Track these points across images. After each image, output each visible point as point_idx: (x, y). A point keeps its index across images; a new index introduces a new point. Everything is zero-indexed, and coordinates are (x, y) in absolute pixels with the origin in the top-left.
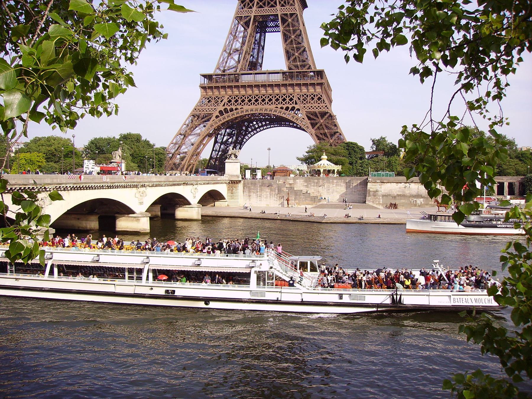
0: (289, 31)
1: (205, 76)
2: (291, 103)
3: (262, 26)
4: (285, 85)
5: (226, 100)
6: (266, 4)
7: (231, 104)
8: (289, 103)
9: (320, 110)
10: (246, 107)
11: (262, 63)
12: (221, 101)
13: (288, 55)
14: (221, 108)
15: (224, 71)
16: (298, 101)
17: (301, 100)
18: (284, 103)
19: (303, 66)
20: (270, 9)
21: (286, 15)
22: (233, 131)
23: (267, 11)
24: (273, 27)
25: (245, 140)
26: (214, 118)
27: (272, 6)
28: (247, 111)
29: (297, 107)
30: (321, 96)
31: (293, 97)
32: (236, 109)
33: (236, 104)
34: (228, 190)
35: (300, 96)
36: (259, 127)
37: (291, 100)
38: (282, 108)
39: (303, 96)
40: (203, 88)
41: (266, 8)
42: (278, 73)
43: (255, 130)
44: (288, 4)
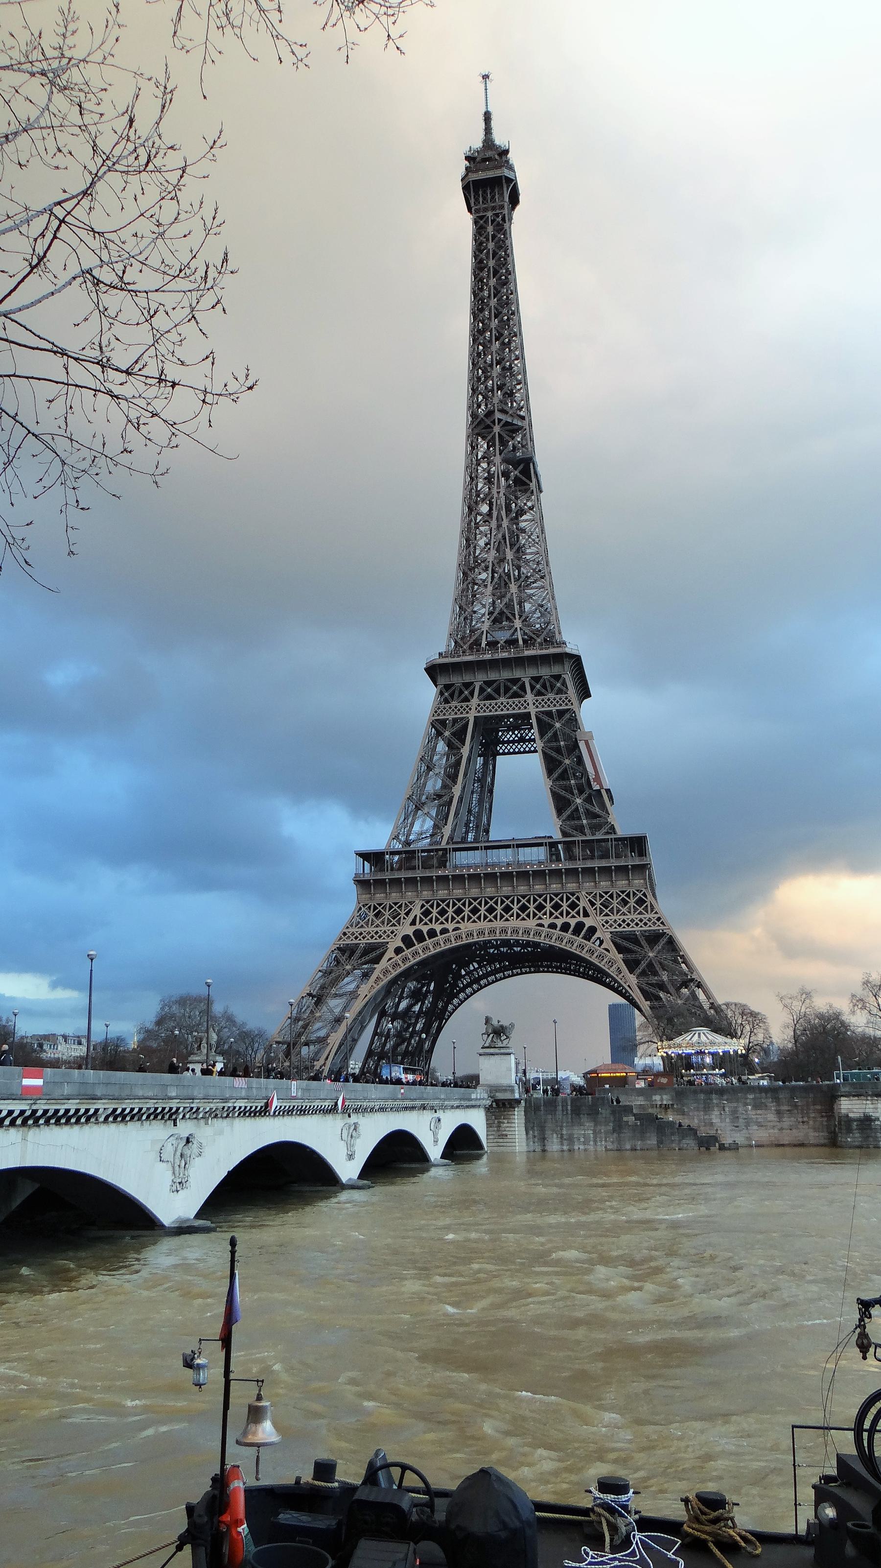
0: (558, 750)
1: (365, 856)
2: (573, 913)
3: (490, 738)
4: (556, 873)
5: (417, 911)
6: (502, 691)
8: (568, 913)
10: (466, 927)
11: (489, 825)
12: (407, 914)
13: (561, 803)
15: (408, 843)
17: (598, 905)
18: (556, 914)
19: (595, 828)
20: (511, 701)
21: (549, 714)
22: (422, 987)
23: (504, 706)
24: (513, 742)
25: (450, 1007)
26: (390, 953)
27: (516, 695)
28: (470, 934)
29: (588, 922)
30: (644, 895)
31: (578, 898)
33: (442, 919)
34: (489, 1126)
35: (595, 897)
36: (485, 976)
37: (573, 906)
38: (553, 926)
40: (362, 883)
41: (502, 699)
42: (540, 845)
43: (477, 983)
44: (552, 690)
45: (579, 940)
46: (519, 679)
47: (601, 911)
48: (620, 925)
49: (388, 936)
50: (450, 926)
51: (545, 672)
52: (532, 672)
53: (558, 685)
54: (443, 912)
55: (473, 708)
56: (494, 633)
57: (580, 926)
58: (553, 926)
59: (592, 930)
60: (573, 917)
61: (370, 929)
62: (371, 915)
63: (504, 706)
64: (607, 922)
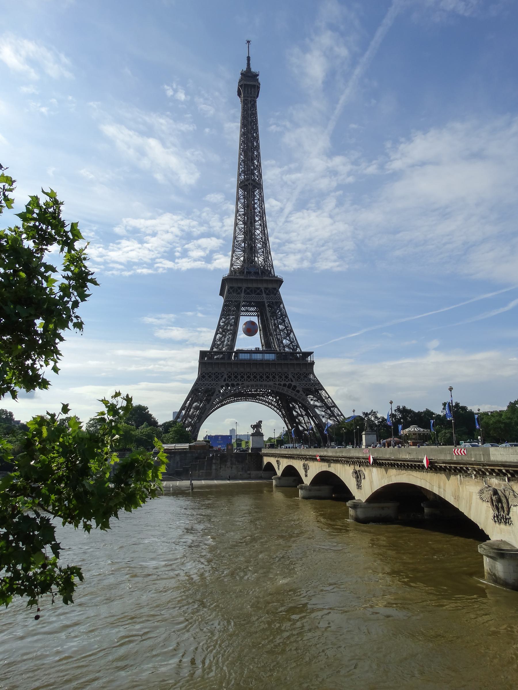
5: (226, 376)
7: (232, 380)
8: (285, 380)
12: (222, 377)
17: (296, 378)
27: (258, 294)
29: (293, 384)
31: (288, 374)
33: (236, 380)
39: (297, 374)
41: (253, 295)
47: (298, 380)
50: (240, 383)
51: (270, 286)
52: (265, 285)
54: (236, 377)
58: (280, 385)
61: (207, 382)
62: (207, 377)
63: (254, 297)
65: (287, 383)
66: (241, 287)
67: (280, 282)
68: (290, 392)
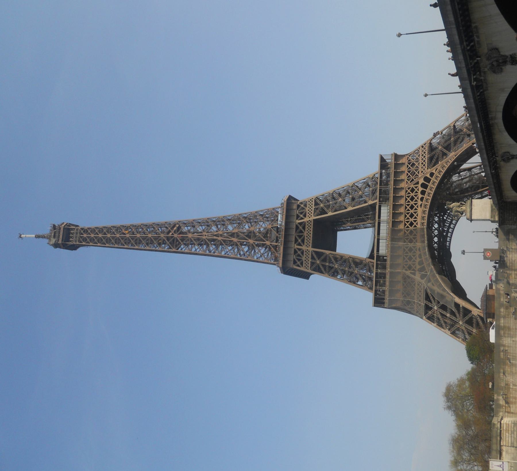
2: (416, 190)
5: (408, 273)
6: (301, 234)
7: (414, 264)
8: (416, 192)
9: (427, 152)
12: (409, 277)
14: (417, 277)
16: (416, 181)
18: (416, 198)
20: (306, 229)
21: (316, 209)
27: (304, 228)
29: (421, 181)
31: (409, 189)
32: (420, 256)
33: (414, 258)
37: (412, 190)
41: (305, 234)
45: (430, 185)
46: (297, 226)
47: (417, 175)
48: (424, 165)
49: (420, 287)
50: (418, 253)
53: (302, 206)
55: (307, 248)
56: (272, 239)
57: (424, 186)
58: (422, 199)
59: (427, 179)
60: (418, 190)
64: (422, 172)
65: (421, 189)
66: (295, 250)
67: (290, 200)
68: (433, 186)
